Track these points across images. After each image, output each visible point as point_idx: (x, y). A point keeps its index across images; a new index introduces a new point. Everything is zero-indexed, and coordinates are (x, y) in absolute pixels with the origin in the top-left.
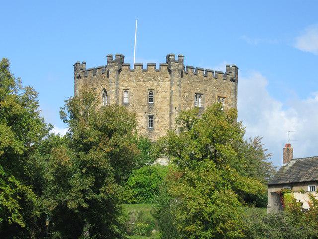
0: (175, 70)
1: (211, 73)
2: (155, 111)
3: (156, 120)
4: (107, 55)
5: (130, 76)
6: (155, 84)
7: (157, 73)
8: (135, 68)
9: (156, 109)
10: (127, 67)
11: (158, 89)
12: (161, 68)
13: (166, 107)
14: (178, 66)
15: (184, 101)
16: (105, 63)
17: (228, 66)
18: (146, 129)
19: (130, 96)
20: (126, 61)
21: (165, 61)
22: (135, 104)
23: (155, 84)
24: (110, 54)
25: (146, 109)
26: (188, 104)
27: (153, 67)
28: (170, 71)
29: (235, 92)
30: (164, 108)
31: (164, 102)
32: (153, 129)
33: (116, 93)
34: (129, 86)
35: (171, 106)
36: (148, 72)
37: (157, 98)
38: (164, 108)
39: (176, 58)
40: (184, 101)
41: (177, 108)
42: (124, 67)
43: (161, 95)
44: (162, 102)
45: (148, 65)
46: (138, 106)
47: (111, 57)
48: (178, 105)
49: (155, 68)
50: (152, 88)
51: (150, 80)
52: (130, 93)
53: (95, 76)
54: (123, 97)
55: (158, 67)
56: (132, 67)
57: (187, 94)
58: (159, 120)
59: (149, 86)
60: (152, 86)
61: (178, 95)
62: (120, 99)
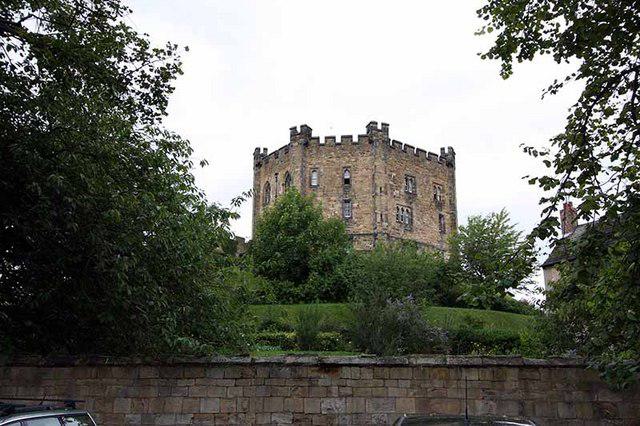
3: (355, 205)
5: (318, 151)
17: (443, 149)
19: (320, 176)
20: (314, 135)
24: (293, 126)
25: (341, 191)
28: (371, 142)
29: (452, 179)
32: (351, 218)
33: (302, 172)
35: (375, 186)
39: (379, 127)
42: (312, 141)
47: (293, 129)
55: (355, 139)
56: (322, 141)
59: (344, 162)
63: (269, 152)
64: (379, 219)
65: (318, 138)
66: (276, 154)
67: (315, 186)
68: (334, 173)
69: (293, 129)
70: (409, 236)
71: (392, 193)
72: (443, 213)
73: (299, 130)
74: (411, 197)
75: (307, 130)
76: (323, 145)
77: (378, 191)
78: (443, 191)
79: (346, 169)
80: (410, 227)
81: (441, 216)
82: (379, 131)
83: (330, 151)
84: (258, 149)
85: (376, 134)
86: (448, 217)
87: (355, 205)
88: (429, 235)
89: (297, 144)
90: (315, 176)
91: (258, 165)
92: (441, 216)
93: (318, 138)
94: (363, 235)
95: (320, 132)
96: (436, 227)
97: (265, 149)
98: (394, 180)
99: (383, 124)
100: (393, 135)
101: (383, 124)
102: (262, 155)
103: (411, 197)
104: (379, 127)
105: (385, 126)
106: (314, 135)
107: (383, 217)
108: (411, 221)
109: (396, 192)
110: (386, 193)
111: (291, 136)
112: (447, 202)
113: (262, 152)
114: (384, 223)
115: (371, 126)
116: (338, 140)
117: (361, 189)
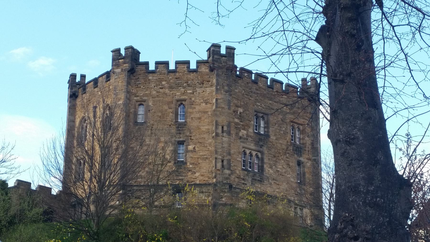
0: (221, 68)
1: (278, 85)
2: (188, 134)
3: (190, 147)
4: (112, 49)
6: (188, 92)
7: (192, 75)
8: (156, 68)
9: (189, 130)
10: (143, 68)
11: (193, 99)
12: (197, 67)
13: (207, 127)
14: (226, 62)
15: (236, 120)
16: (109, 68)
18: (173, 162)
19: (148, 111)
20: (142, 59)
21: (204, 56)
22: (155, 123)
23: (188, 92)
24: (117, 47)
25: (173, 130)
26: (243, 125)
27: (186, 66)
30: (204, 129)
31: (203, 118)
34: (146, 95)
36: (177, 74)
37: (190, 113)
38: (204, 129)
39: (223, 51)
40: (236, 120)
41: (225, 128)
42: (140, 67)
43: (198, 108)
44: (200, 118)
45: (177, 63)
46: (160, 126)
47: (117, 52)
48: (225, 123)
49: (189, 67)
50: (183, 97)
51: (178, 85)
52: (148, 106)
53: (96, 89)
54: (136, 114)
56: (152, 67)
57: (241, 110)
58: (194, 148)
60: (184, 94)
61: (226, 107)
62: (132, 116)
63: (87, 80)
64: (219, 165)
65: (146, 64)
66: (95, 81)
67: (142, 124)
68: (166, 107)
69: (117, 52)
70: (259, 188)
71: (237, 134)
72: (301, 159)
73: (123, 52)
74: (262, 140)
75: (133, 54)
76: (153, 72)
77: (220, 130)
78: (302, 132)
79: (181, 102)
80: (260, 176)
81: (299, 163)
82: (223, 56)
83: (161, 80)
84: (73, 76)
85: (220, 60)
86: (309, 164)
87: (190, 147)
88: (284, 186)
89: (118, 70)
90: (141, 110)
91: (73, 96)
92: (299, 163)
93: (146, 64)
94: (200, 185)
95: (149, 56)
96: (292, 178)
97: (83, 77)
98: (241, 117)
99: (228, 48)
100: (240, 62)
101: (228, 48)
102: (79, 84)
103: (262, 140)
104: (223, 51)
105: (231, 50)
106: (142, 59)
107: (225, 163)
108: (261, 169)
109: (243, 133)
110: (229, 133)
111: (114, 60)
112: (308, 146)
113: (78, 79)
114: (227, 172)
115: (214, 49)
116: (172, 67)
117: (198, 128)
